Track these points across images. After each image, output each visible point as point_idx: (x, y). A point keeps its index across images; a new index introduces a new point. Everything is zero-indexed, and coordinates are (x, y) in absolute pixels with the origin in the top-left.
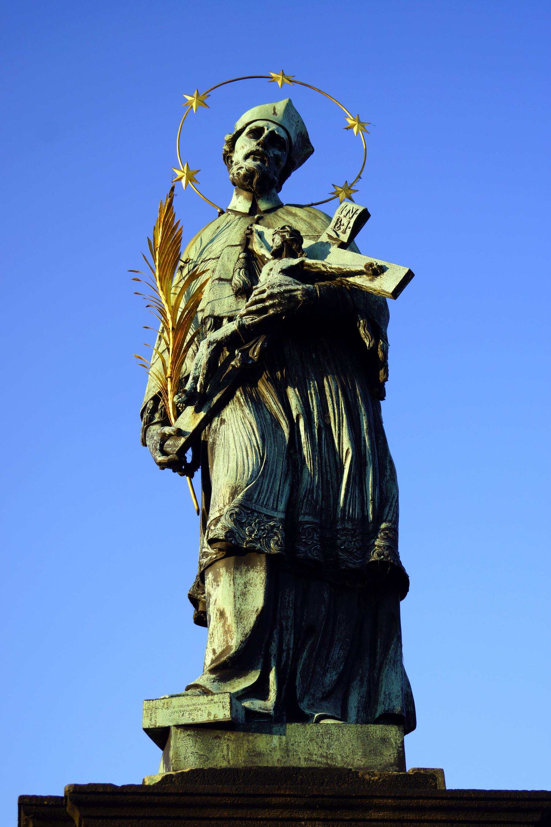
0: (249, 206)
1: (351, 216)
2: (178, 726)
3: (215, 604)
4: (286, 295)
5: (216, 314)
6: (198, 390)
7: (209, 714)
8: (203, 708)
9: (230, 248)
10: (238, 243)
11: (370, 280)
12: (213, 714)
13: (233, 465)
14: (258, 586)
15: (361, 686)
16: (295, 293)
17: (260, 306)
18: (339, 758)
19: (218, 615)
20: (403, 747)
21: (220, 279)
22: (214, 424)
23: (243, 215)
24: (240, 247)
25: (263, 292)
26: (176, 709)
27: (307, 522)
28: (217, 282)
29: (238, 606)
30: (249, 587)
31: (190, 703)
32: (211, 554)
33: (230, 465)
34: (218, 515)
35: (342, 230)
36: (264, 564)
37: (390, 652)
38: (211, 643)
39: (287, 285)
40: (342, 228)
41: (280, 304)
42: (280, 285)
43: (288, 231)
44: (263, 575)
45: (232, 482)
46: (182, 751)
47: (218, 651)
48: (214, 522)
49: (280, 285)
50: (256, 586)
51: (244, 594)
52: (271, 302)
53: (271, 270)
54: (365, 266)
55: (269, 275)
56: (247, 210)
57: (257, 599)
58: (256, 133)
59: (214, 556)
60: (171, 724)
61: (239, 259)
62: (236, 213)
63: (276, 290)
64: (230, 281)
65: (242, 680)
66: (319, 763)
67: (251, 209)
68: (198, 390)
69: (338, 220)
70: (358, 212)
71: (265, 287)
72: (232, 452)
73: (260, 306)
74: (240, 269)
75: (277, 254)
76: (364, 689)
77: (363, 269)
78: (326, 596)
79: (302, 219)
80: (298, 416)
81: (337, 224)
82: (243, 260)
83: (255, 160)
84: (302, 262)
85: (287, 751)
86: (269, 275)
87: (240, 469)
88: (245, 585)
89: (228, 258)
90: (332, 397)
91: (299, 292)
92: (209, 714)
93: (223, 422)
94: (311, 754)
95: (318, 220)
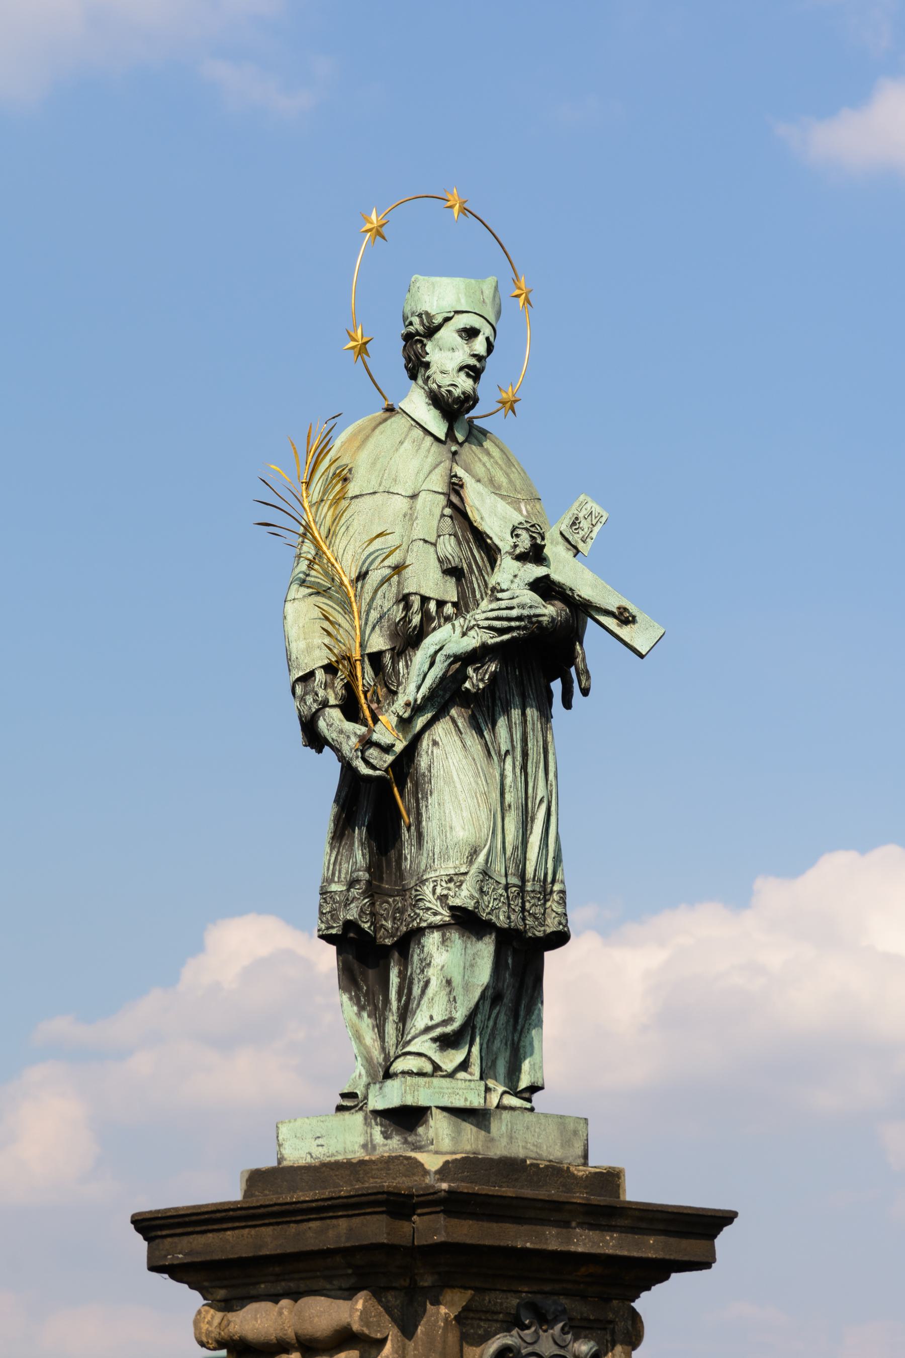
0: (445, 430)
1: (594, 523)
2: (437, 1107)
3: (441, 970)
4: (534, 619)
5: (423, 592)
6: (419, 702)
7: (466, 1100)
8: (461, 1093)
9: (431, 496)
10: (440, 490)
11: (618, 625)
12: (469, 1099)
13: (466, 814)
14: (485, 959)
15: (506, 1049)
16: (541, 619)
17: (505, 624)
18: (545, 1148)
19: (444, 981)
20: (587, 1140)
21: (425, 541)
22: (425, 743)
23: (437, 439)
24: (442, 497)
25: (512, 608)
26: (437, 1090)
27: (515, 886)
28: (421, 542)
29: (466, 977)
30: (477, 959)
31: (449, 1085)
32: (442, 914)
33: (464, 815)
34: (452, 872)
35: (580, 536)
36: (493, 937)
37: (534, 1017)
38: (428, 1008)
39: (537, 607)
40: (582, 533)
41: (524, 628)
42: (531, 607)
43: (539, 533)
44: (492, 948)
45: (472, 840)
46: (440, 1131)
47: (438, 1019)
48: (447, 878)
49: (531, 607)
50: (483, 958)
51: (472, 966)
52: (517, 623)
53: (515, 576)
54: (619, 608)
55: (512, 582)
56: (442, 436)
57: (483, 974)
58: (470, 333)
59: (447, 919)
60: (432, 1105)
61: (443, 516)
62: (427, 432)
63: (526, 612)
64: (435, 545)
65: (453, 1051)
66: (532, 1151)
67: (447, 435)
68: (419, 702)
69: (577, 518)
70: (603, 520)
71: (514, 602)
72: (461, 797)
73: (505, 624)
74: (450, 535)
75: (522, 558)
76: (508, 1054)
77: (615, 610)
78: (510, 961)
79: (497, 463)
80: (507, 752)
81: (574, 524)
82: (449, 520)
83: (468, 375)
84: (547, 577)
85: (511, 1138)
86: (512, 582)
87: (476, 824)
88: (475, 955)
89: (430, 510)
90: (533, 730)
91: (545, 618)
92: (466, 1100)
93: (435, 743)
94: (526, 1142)
95: (514, 469)
